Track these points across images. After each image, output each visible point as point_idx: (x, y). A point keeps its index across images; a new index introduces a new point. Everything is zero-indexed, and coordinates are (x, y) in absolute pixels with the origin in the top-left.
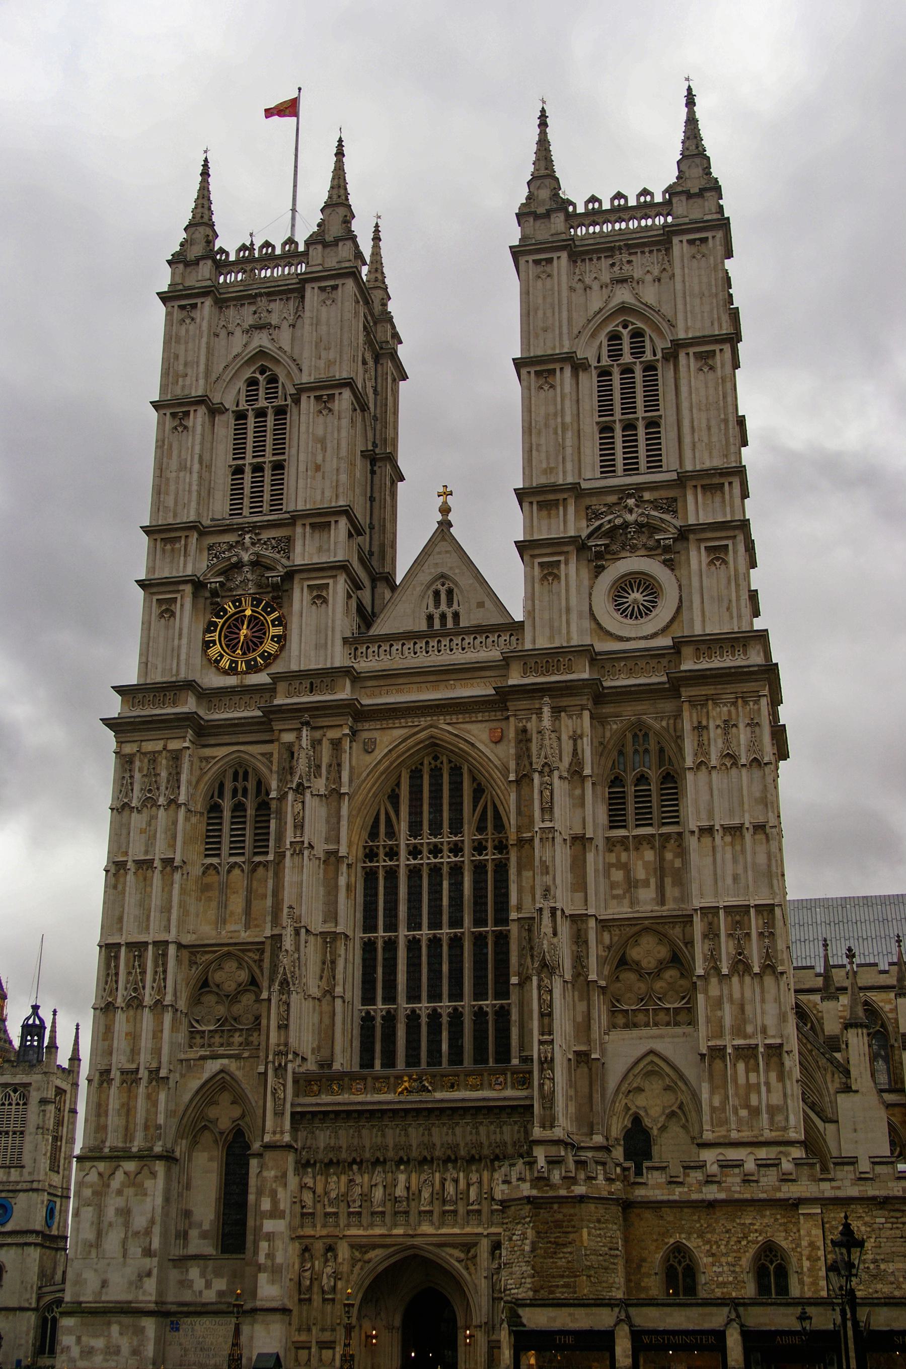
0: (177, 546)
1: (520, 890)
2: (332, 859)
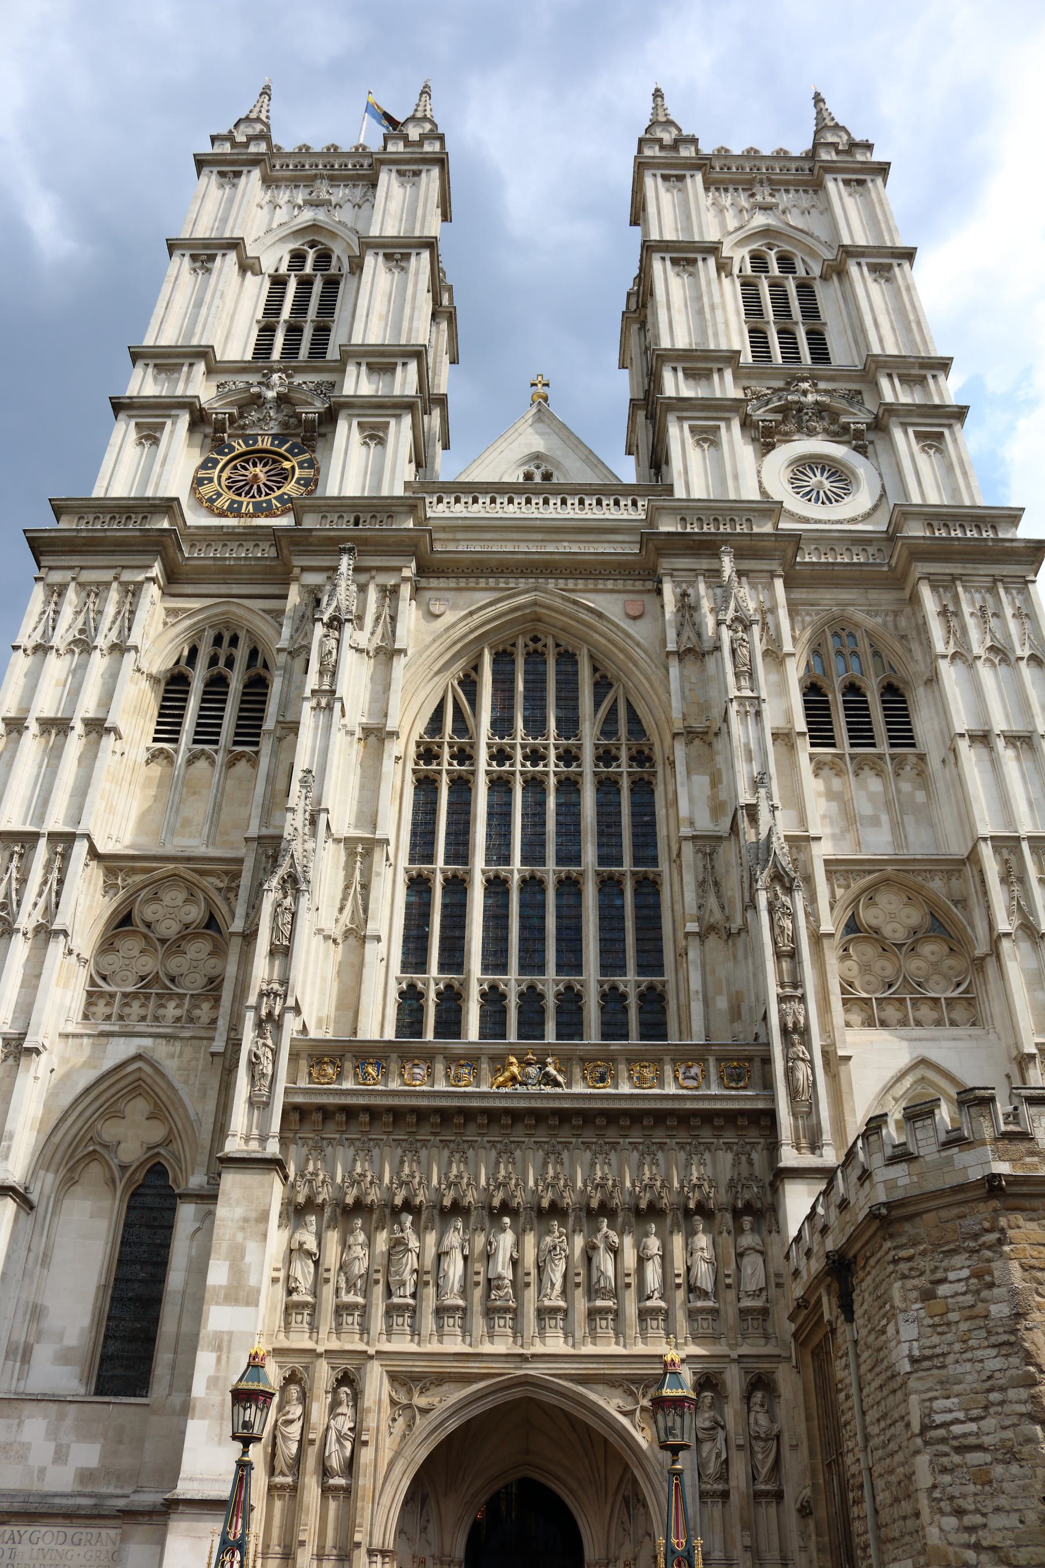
0: (176, 375)
1: (691, 800)
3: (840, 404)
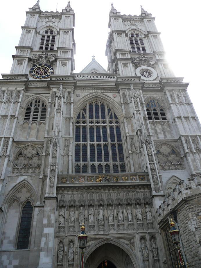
0: (25, 52)
2: (68, 119)
3: (148, 59)
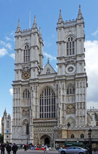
2: (36, 98)
